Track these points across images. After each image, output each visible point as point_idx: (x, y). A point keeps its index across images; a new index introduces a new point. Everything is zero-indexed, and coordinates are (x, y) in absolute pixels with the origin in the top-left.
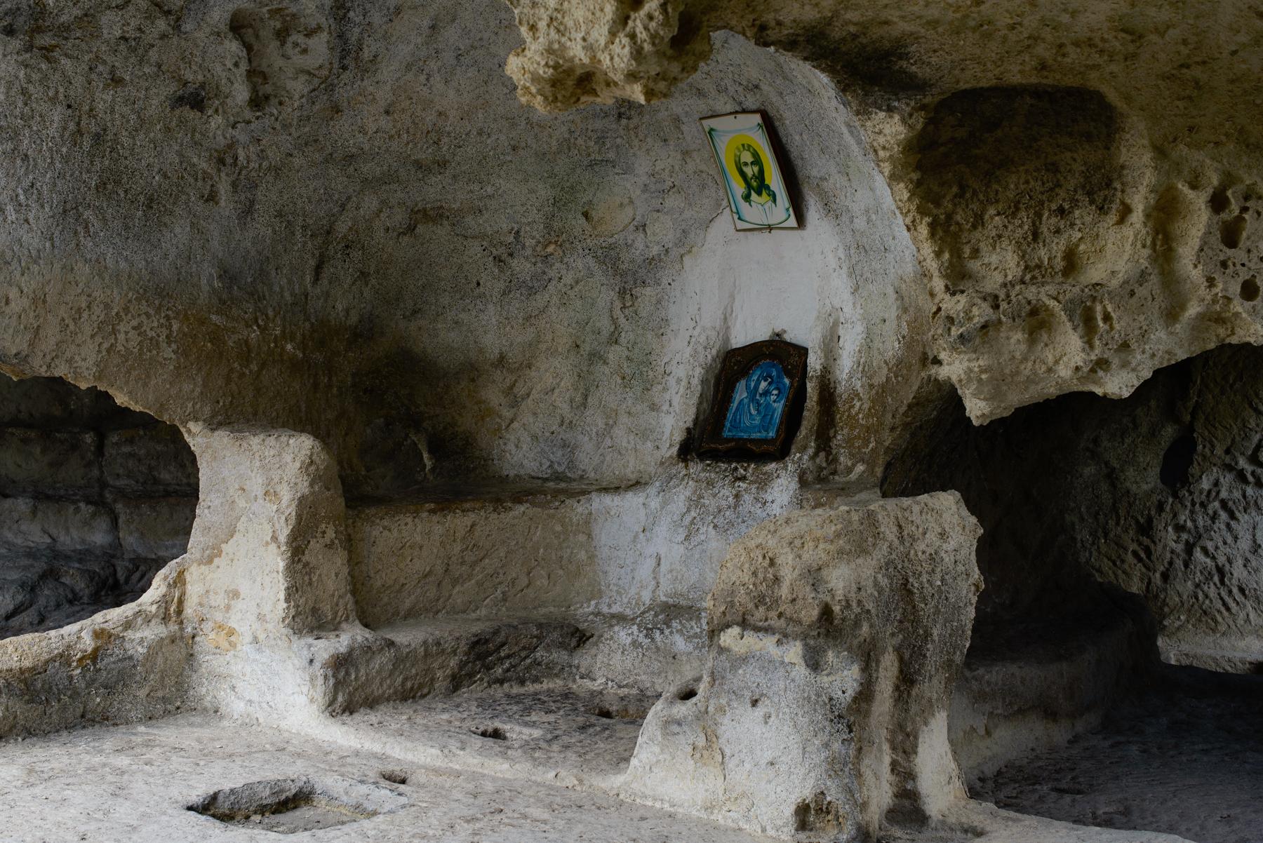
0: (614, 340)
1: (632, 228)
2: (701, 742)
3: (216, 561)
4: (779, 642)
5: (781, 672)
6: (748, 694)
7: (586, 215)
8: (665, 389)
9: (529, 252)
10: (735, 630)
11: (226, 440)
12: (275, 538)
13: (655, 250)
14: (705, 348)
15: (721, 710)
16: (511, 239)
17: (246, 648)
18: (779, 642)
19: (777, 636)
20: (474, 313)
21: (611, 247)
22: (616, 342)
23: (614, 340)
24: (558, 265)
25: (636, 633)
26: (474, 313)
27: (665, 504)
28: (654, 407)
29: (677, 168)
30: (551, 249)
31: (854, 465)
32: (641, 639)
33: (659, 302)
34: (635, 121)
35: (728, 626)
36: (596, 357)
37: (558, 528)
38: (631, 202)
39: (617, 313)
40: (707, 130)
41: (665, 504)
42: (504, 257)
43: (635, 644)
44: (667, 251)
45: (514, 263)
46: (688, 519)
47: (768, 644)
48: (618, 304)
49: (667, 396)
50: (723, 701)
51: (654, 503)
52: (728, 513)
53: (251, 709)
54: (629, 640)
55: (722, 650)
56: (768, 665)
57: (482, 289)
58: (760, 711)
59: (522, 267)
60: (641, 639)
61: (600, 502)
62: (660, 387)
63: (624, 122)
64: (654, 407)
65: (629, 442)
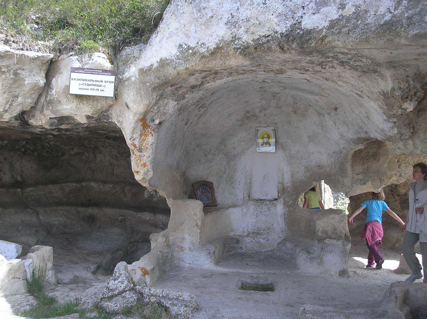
0: (224, 173)
1: (233, 148)
2: (319, 261)
3: (177, 231)
4: (337, 241)
5: (337, 246)
6: (330, 251)
7: (225, 145)
8: (236, 184)
9: (212, 153)
10: (328, 239)
11: (180, 202)
12: (197, 225)
13: (236, 153)
14: (249, 175)
15: (324, 255)
16: (209, 150)
17: (187, 251)
18: (337, 241)
19: (337, 240)
20: (198, 167)
21: (228, 153)
22: (225, 173)
23: (224, 173)
24: (217, 156)
25: (250, 239)
26: (198, 167)
27: (248, 210)
28: (233, 188)
29: (246, 136)
30: (216, 153)
31: (290, 201)
32: (252, 240)
33: (235, 164)
34: (242, 127)
35: (326, 239)
36: (221, 177)
37: (225, 216)
38: (234, 143)
39: (226, 167)
40: (257, 130)
41: (248, 210)
42: (207, 154)
43: (251, 241)
44: (238, 154)
45: (208, 156)
46: (255, 213)
47: (334, 242)
48: (227, 165)
49: (236, 185)
50: (324, 253)
51: (245, 210)
52: (267, 212)
53: (191, 265)
54: (249, 241)
55: (324, 243)
56: (334, 245)
57: (200, 161)
58: (332, 254)
59: (210, 157)
60: (252, 240)
61: (231, 210)
62: (235, 183)
63: (240, 127)
64: (233, 188)
65: (228, 196)
